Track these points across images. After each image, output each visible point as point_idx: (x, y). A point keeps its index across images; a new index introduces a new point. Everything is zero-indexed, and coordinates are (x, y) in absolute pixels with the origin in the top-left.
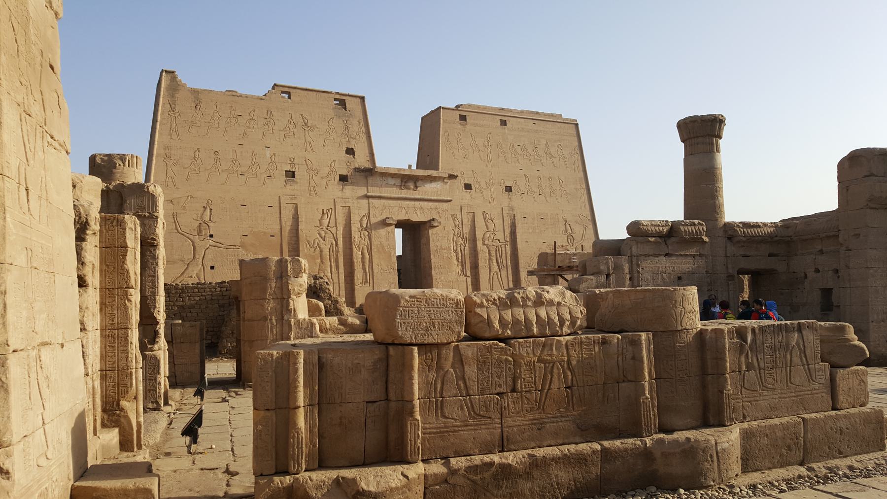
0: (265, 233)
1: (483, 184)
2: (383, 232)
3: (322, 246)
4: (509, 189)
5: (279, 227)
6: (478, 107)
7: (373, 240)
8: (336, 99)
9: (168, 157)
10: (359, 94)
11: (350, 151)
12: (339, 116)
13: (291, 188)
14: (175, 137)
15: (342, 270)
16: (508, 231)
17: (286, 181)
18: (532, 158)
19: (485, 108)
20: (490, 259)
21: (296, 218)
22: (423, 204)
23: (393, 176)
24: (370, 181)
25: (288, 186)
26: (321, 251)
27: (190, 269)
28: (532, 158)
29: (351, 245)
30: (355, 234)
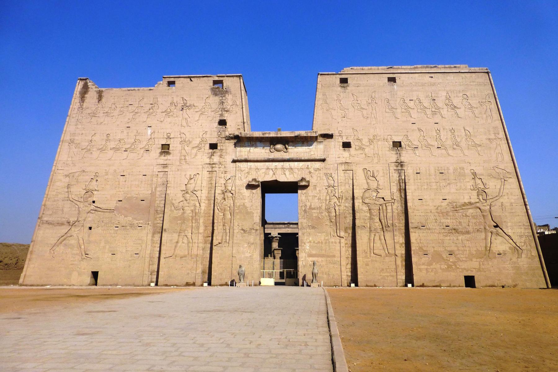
0: (137, 198)
1: (365, 141)
4: (397, 145)
7: (236, 201)
9: (72, 141)
11: (223, 123)
12: (216, 95)
13: (163, 159)
14: (80, 126)
15: (201, 230)
16: (395, 189)
17: (161, 153)
18: (429, 112)
20: (371, 218)
22: (292, 164)
25: (162, 157)
26: (184, 213)
27: (73, 229)
28: (426, 110)
30: (219, 197)
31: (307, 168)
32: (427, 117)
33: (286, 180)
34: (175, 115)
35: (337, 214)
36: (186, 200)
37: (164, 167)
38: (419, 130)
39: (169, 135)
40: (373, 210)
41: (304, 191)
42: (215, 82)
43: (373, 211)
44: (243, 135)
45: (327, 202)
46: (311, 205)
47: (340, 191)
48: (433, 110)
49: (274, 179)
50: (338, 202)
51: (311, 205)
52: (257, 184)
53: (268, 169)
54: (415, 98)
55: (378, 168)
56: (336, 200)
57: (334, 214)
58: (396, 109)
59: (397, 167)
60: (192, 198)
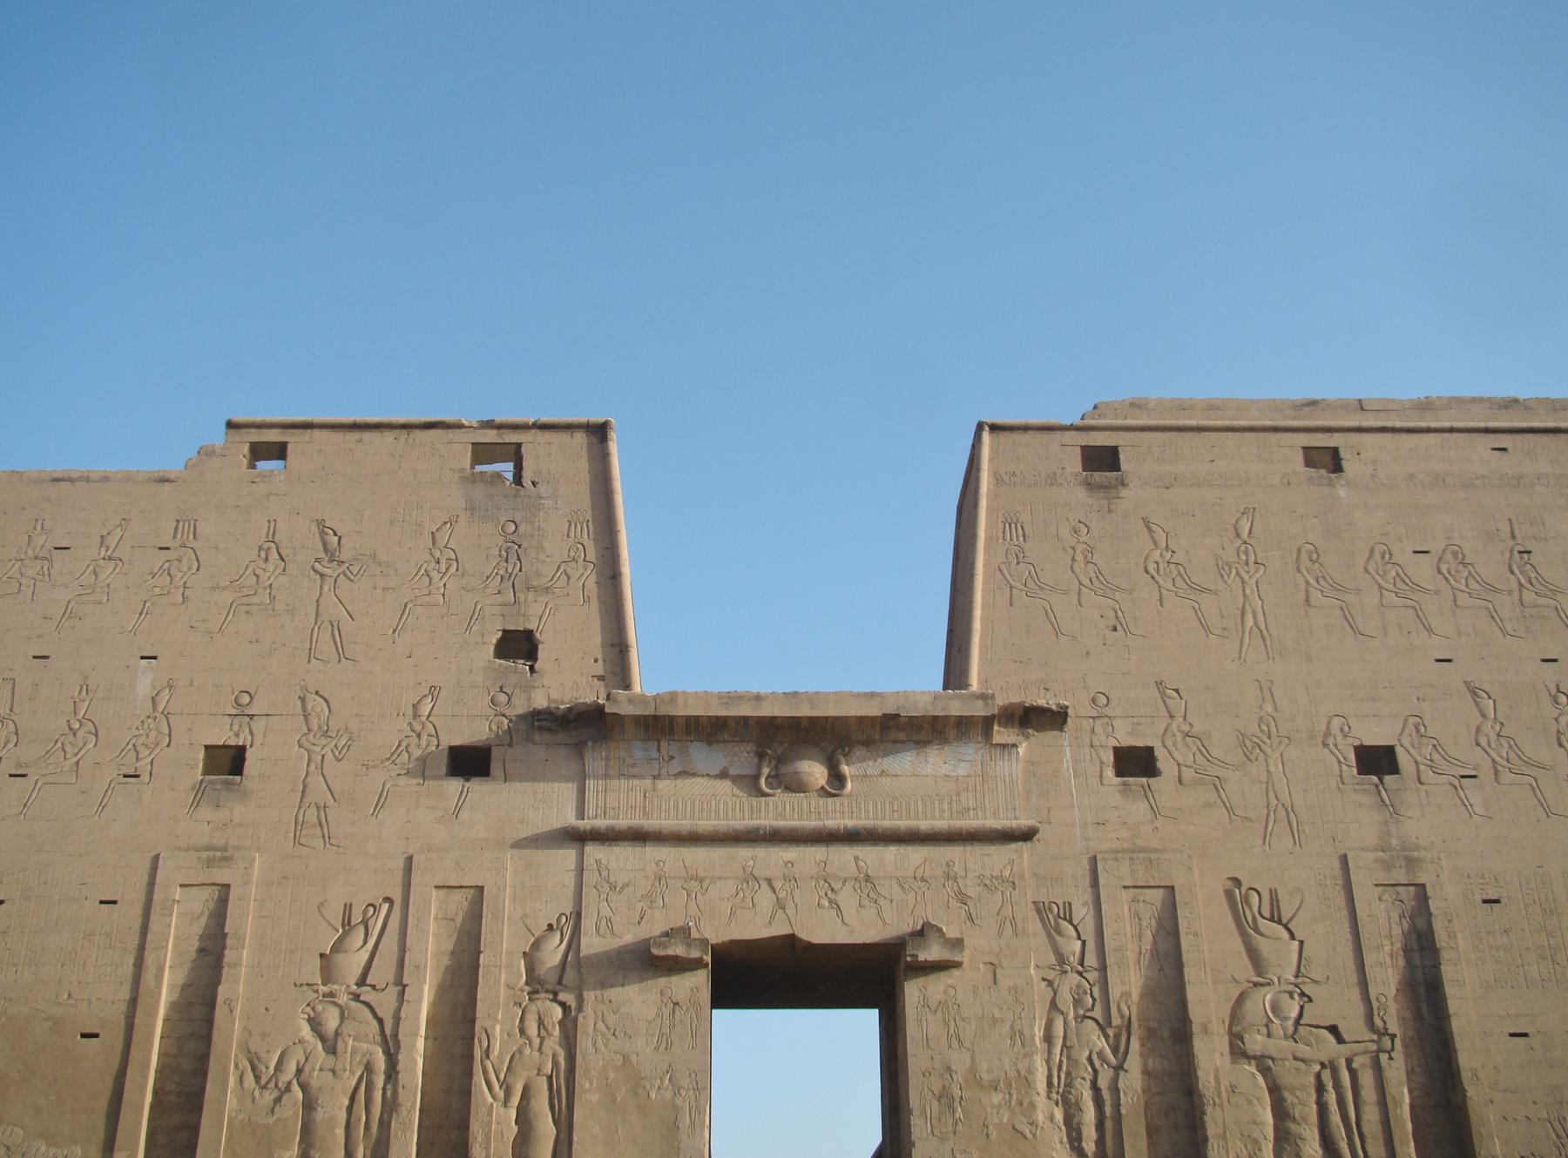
2: (638, 999)
3: (316, 1079)
4: (1377, 761)
5: (125, 993)
6: (1181, 406)
7: (584, 1044)
8: (482, 453)
10: (582, 418)
11: (519, 645)
16: (1387, 979)
17: (199, 793)
19: (1212, 407)
21: (211, 954)
22: (869, 854)
23: (712, 730)
24: (594, 760)
25: (205, 812)
26: (309, 1105)
29: (469, 1074)
31: (947, 876)
32: (1505, 633)
33: (841, 937)
34: (280, 606)
35: (1108, 1110)
36: (322, 1038)
37: (210, 863)
38: (1474, 693)
39: (246, 699)
40: (1292, 1091)
41: (935, 986)
42: (482, 453)
43: (1287, 1095)
44: (625, 709)
45: (1057, 1050)
46: (973, 1070)
47: (1115, 993)
48: (1528, 596)
49: (779, 929)
50: (1108, 1051)
51: (973, 1070)
52: (695, 954)
53: (750, 878)
54: (1436, 546)
55: (1301, 878)
56: (1101, 1044)
57: (1089, 1115)
58: (1358, 591)
59: (1387, 866)
60: (349, 1028)
